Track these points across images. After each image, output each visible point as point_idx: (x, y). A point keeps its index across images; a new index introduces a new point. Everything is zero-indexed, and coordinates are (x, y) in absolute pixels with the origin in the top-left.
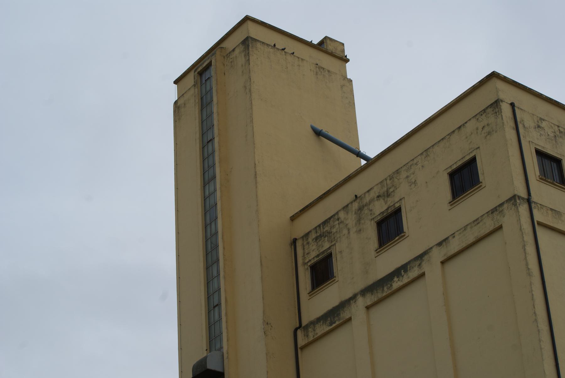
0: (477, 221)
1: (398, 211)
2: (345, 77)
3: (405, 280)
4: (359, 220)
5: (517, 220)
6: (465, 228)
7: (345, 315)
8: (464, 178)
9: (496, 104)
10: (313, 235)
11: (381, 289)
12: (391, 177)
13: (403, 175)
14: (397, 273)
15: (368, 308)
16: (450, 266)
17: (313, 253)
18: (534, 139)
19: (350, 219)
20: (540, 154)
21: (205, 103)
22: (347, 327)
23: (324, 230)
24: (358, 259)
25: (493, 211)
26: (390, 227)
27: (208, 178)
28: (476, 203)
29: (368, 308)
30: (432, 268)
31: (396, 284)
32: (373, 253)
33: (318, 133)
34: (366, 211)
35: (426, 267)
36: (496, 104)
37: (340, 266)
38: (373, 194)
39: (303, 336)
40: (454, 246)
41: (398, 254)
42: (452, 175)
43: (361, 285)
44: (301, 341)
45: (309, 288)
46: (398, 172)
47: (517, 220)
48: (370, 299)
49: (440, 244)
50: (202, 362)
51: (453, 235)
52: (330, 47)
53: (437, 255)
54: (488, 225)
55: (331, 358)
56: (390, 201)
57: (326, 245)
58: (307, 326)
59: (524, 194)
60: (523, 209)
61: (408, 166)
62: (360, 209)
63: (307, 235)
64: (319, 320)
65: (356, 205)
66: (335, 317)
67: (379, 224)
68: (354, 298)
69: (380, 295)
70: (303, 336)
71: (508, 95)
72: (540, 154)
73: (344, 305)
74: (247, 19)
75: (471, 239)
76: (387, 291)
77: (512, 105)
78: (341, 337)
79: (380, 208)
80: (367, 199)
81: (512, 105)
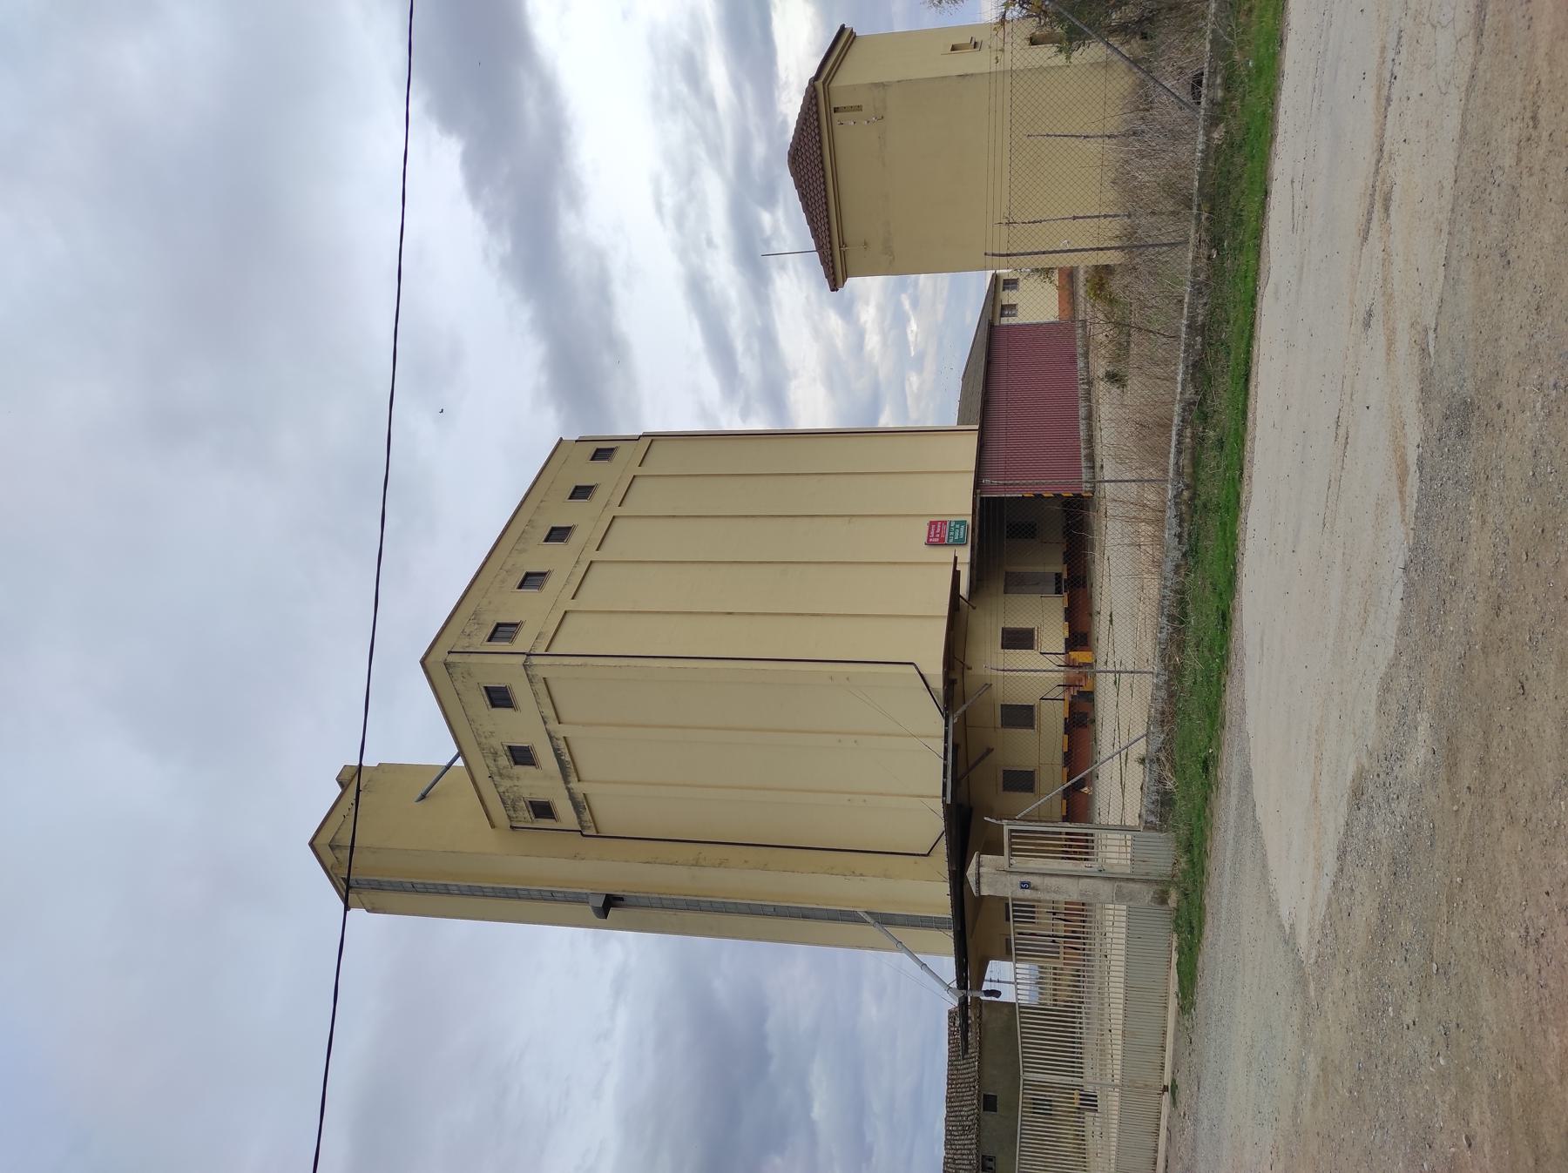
2: (375, 769)
7: (580, 797)
10: (512, 813)
11: (567, 769)
14: (558, 756)
16: (563, 717)
17: (525, 815)
18: (479, 640)
19: (506, 784)
21: (379, 886)
22: (591, 799)
23: (509, 803)
24: (540, 782)
25: (531, 681)
26: (521, 756)
27: (446, 890)
30: (561, 731)
33: (423, 797)
35: (560, 735)
37: (541, 796)
38: (491, 764)
40: (550, 713)
41: (544, 754)
43: (561, 783)
48: (573, 778)
50: (596, 910)
52: (347, 777)
53: (553, 725)
54: (541, 687)
55: (610, 811)
56: (501, 752)
60: (535, 660)
61: (476, 735)
62: (501, 775)
65: (497, 778)
67: (516, 763)
68: (569, 790)
70: (588, 829)
71: (440, 654)
73: (572, 797)
74: (311, 844)
78: (596, 803)
79: (504, 761)
80: (494, 769)
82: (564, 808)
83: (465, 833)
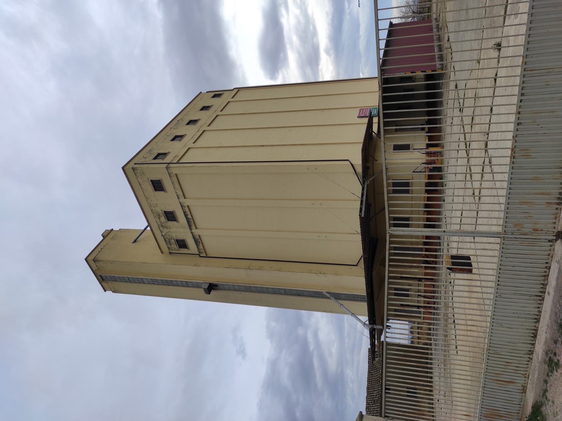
0: (173, 183)
1: (165, 212)
2: (118, 231)
3: (189, 213)
4: (167, 228)
5: (175, 169)
6: (174, 188)
7: (197, 237)
8: (158, 186)
9: (133, 169)
10: (169, 245)
11: (191, 222)
12: (153, 213)
13: (153, 208)
14: (186, 216)
15: (196, 228)
16: (187, 196)
17: (175, 246)
18: (150, 159)
19: (165, 231)
20: (155, 158)
21: (114, 279)
22: (201, 237)
23: (168, 241)
24: (179, 230)
25: (170, 176)
26: (170, 216)
27: (141, 281)
28: (167, 183)
29: (196, 228)
30: (186, 202)
31: (190, 216)
32: (178, 224)
33: (135, 241)
34: (163, 224)
35: (186, 205)
36: (133, 169)
37: (180, 237)
38: (158, 221)
39: (202, 254)
40: (180, 193)
42: (156, 190)
43: (189, 231)
44: (204, 255)
45: (186, 249)
46: (152, 210)
47: (175, 169)
48: (193, 227)
49: (178, 198)
50: (205, 289)
51: (176, 193)
52: (106, 234)
53: (182, 199)
54: (175, 179)
55: (212, 244)
56: (161, 215)
57: (173, 241)
58: (199, 252)
59: (166, 165)
60: (171, 165)
61: (150, 205)
62: (162, 226)
63: (168, 248)
64: (198, 247)
65: (161, 228)
66: (198, 241)
67: (169, 220)
68: (192, 233)
69: (193, 223)
70: (202, 254)
71: (132, 165)
72: (155, 158)
73: (194, 237)
74: (86, 259)
75: (179, 186)
76: (191, 220)
77: (135, 164)
78: (205, 240)
79: (163, 219)
80: (159, 223)
81: (135, 164)
82: (191, 243)
83: (150, 255)
